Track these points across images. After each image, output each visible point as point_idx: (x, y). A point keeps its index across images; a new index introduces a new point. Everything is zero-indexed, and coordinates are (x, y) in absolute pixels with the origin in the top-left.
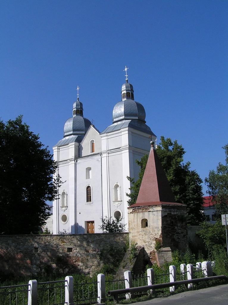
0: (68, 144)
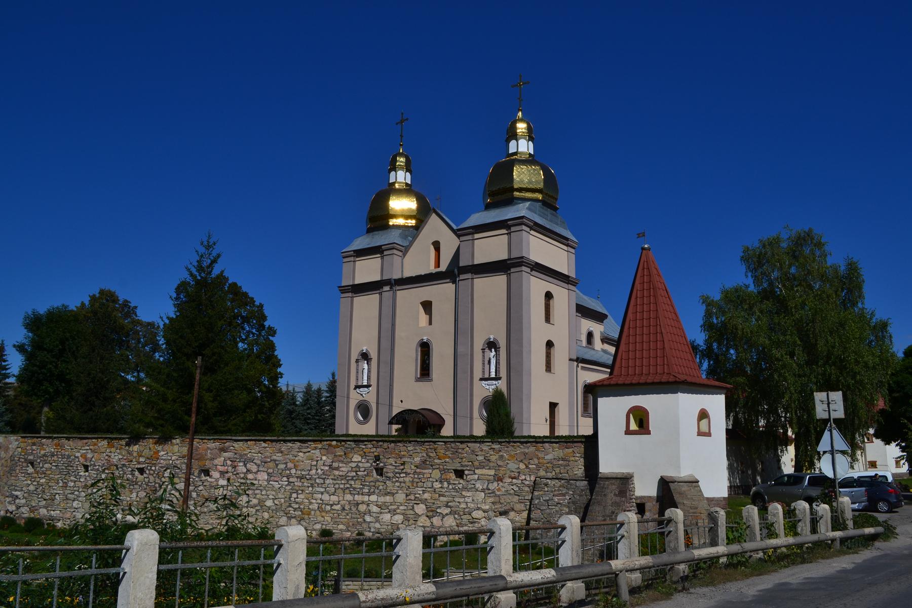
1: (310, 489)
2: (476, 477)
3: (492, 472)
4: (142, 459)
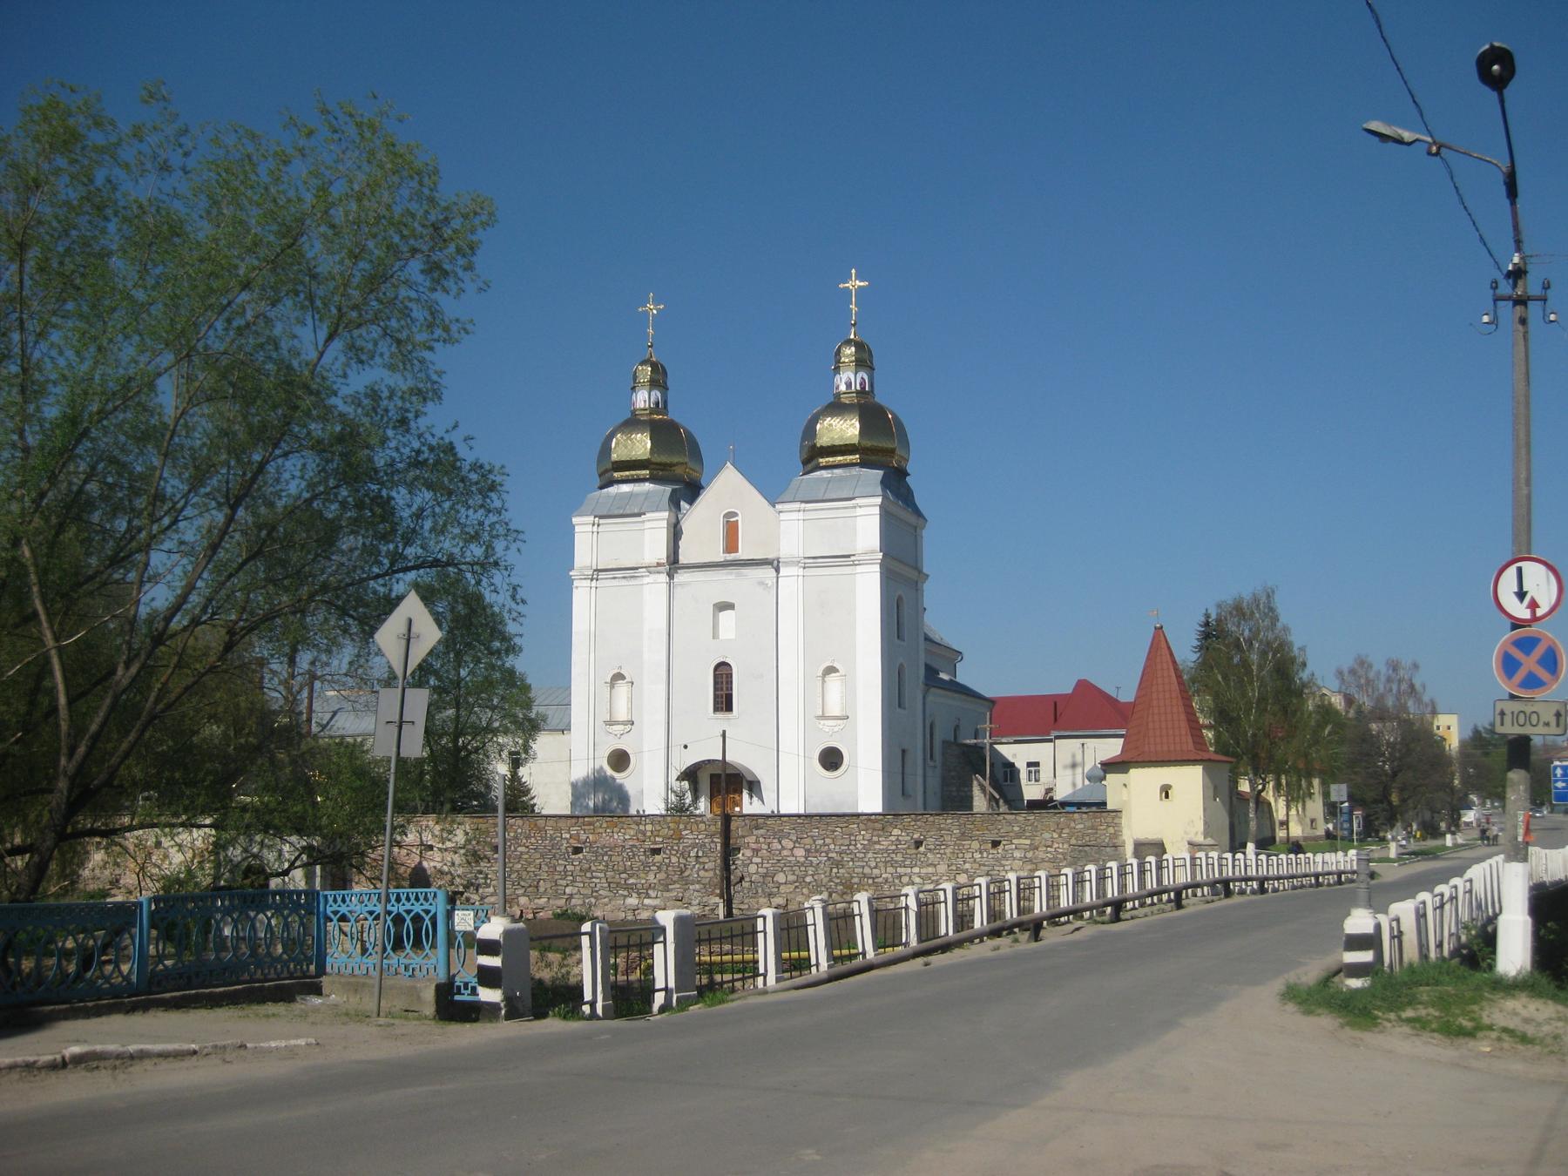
0: (639, 515)
2: (1014, 846)
3: (1028, 842)
4: (657, 839)
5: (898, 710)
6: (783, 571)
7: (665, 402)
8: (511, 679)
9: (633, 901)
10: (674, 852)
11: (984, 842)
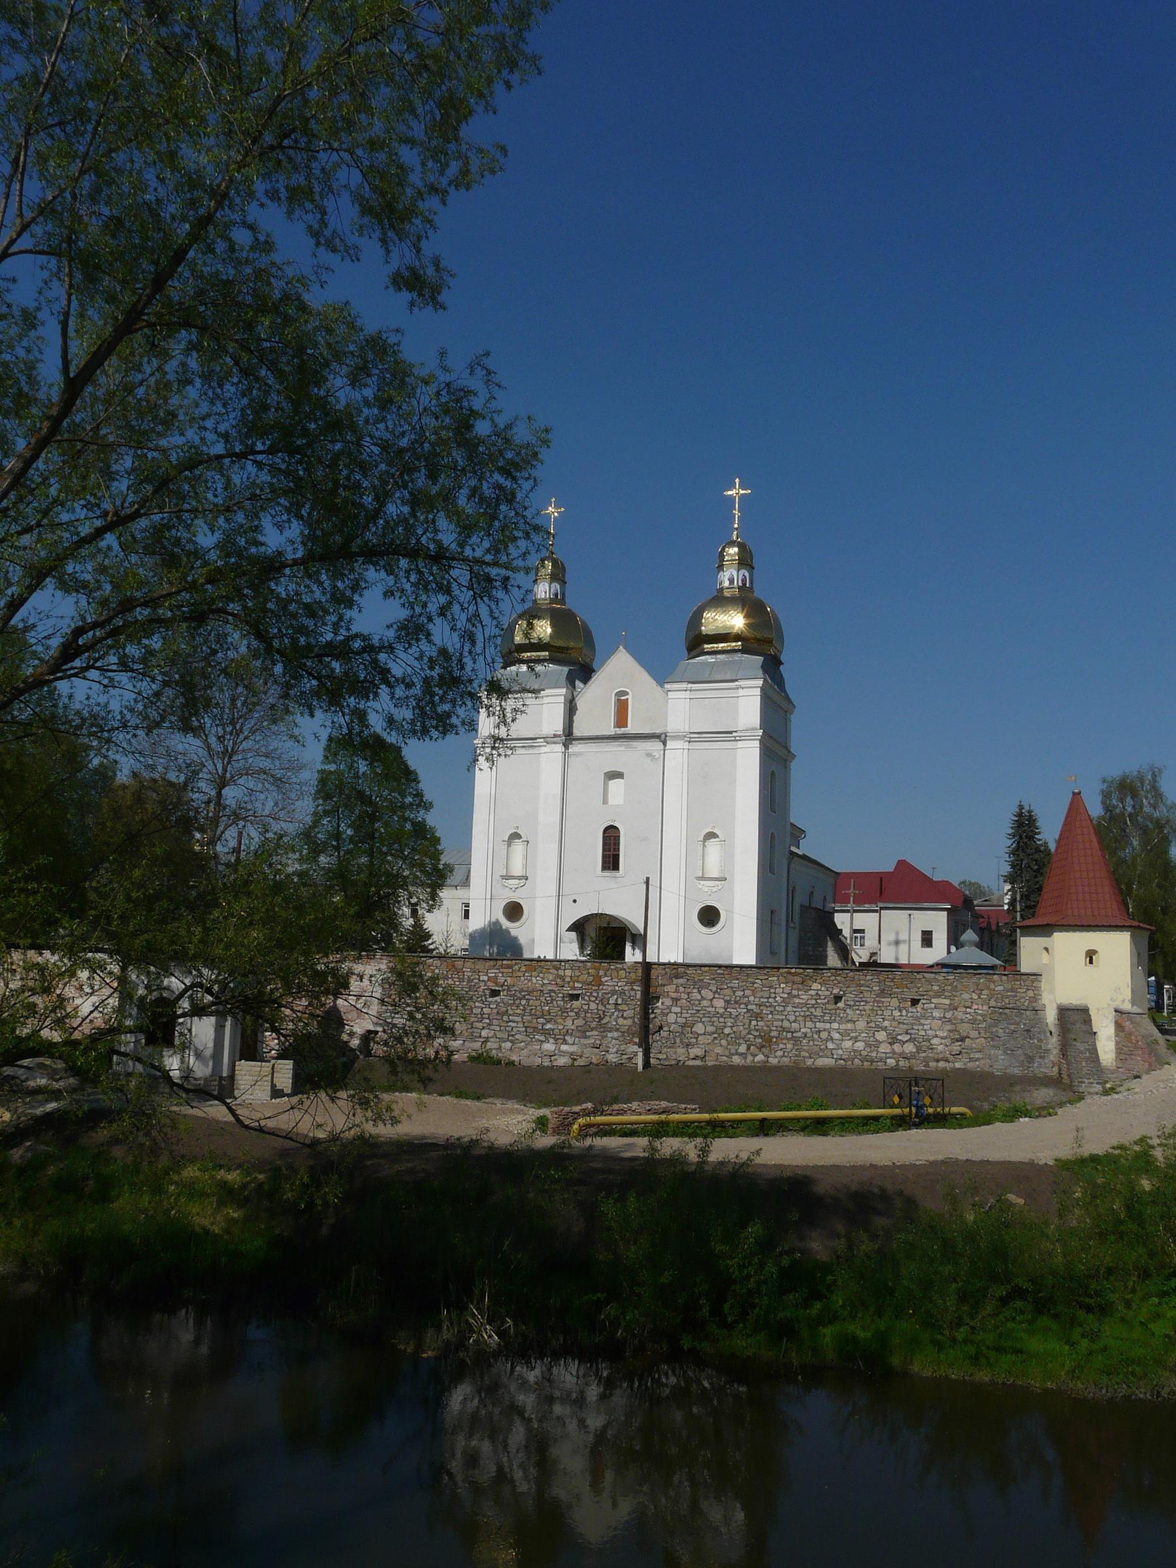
1: (770, 1016)
2: (933, 1006)
3: (947, 1002)
4: (576, 985)
5: (770, 875)
6: (670, 744)
7: (563, 594)
8: (422, 831)
9: (549, 1047)
10: (593, 999)
11: (904, 1000)
